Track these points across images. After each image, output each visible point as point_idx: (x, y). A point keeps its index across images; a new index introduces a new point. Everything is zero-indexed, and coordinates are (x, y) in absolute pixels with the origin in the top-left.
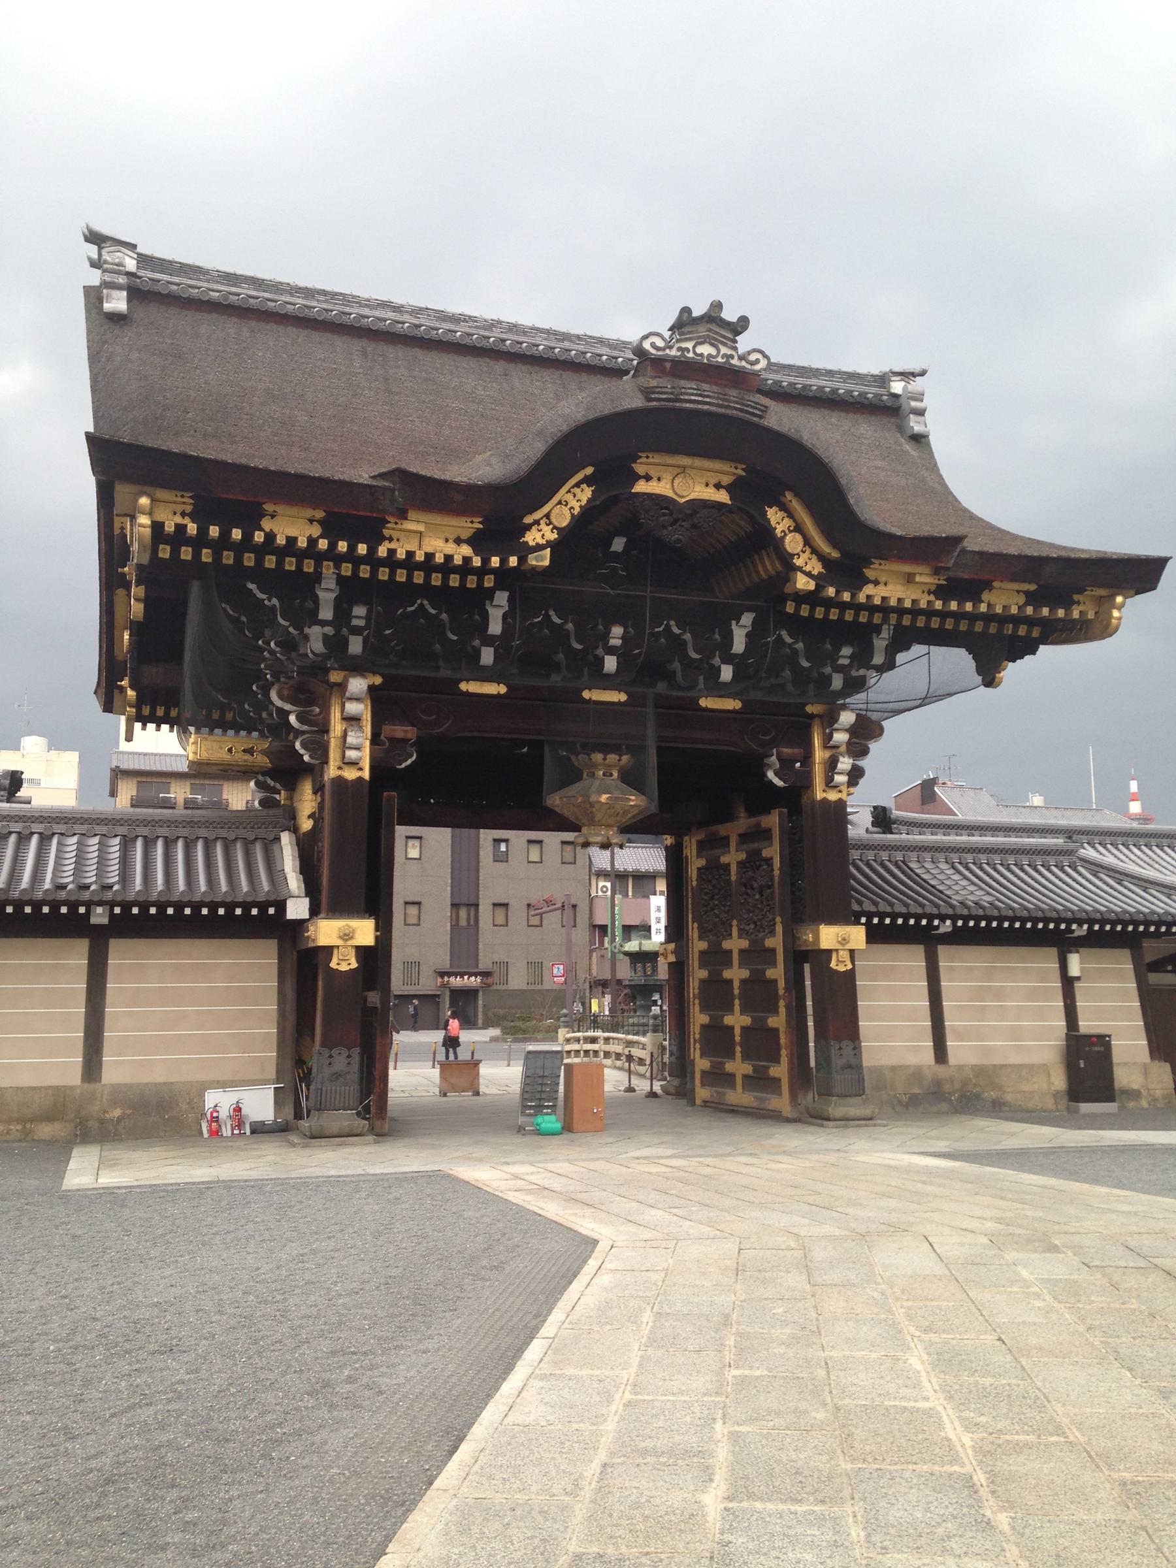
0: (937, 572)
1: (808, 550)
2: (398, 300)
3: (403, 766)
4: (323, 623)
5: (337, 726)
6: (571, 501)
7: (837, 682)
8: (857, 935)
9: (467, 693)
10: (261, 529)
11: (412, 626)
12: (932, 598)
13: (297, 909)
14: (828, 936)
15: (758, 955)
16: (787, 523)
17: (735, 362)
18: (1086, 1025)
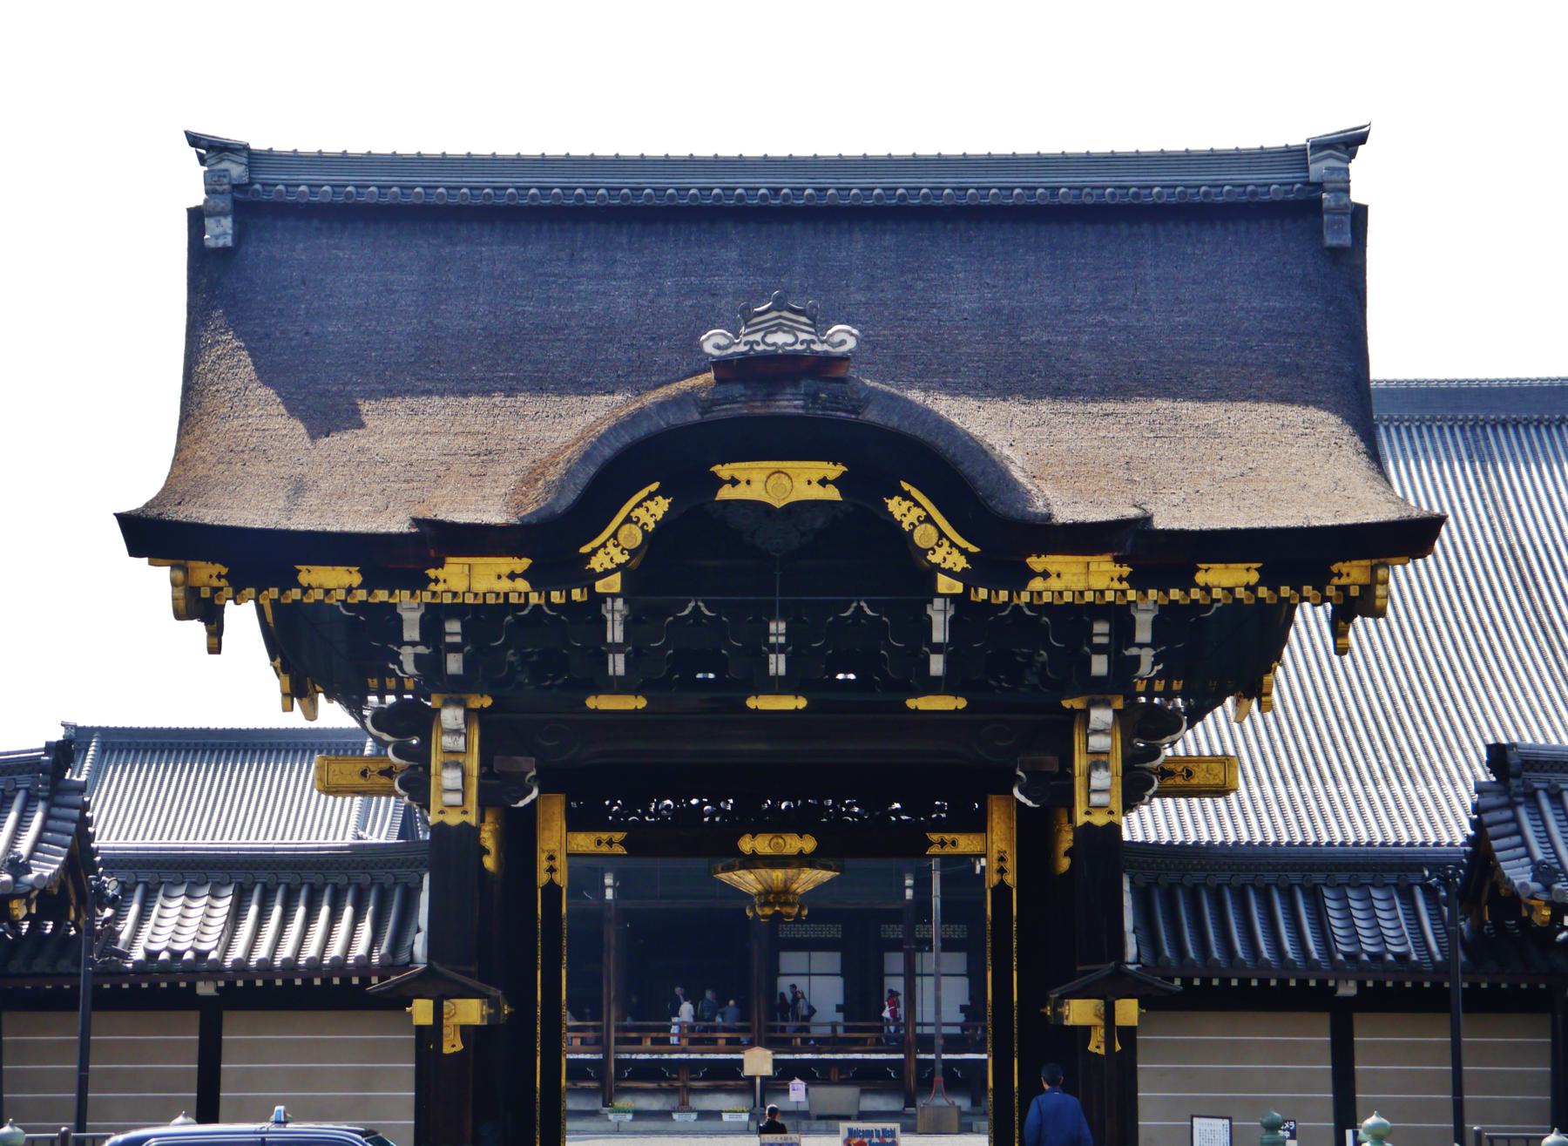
0: (1118, 561)
1: (946, 543)
3: (521, 804)
4: (413, 644)
6: (649, 509)
7: (1100, 665)
9: (596, 711)
10: (298, 585)
12: (1125, 585)
16: (916, 512)
17: (817, 347)
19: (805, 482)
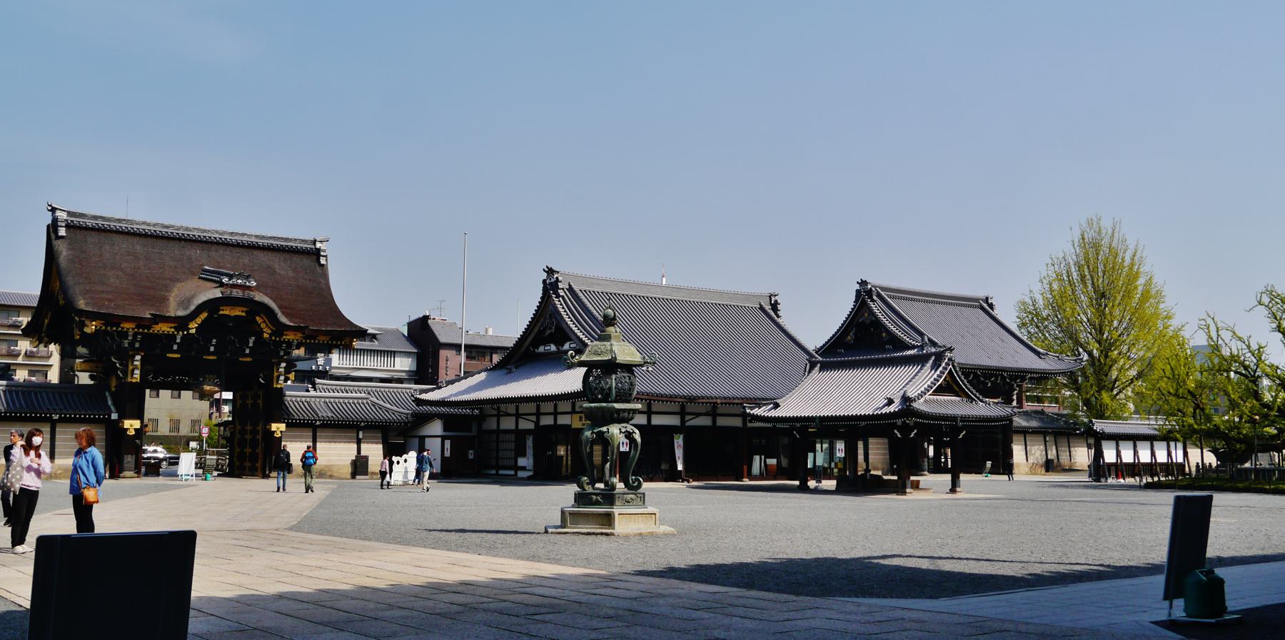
2: (148, 221)
5: (131, 368)
8: (282, 427)
11: (153, 346)
13: (114, 416)
14: (274, 427)
15: (254, 432)
18: (363, 453)
19: (238, 312)
